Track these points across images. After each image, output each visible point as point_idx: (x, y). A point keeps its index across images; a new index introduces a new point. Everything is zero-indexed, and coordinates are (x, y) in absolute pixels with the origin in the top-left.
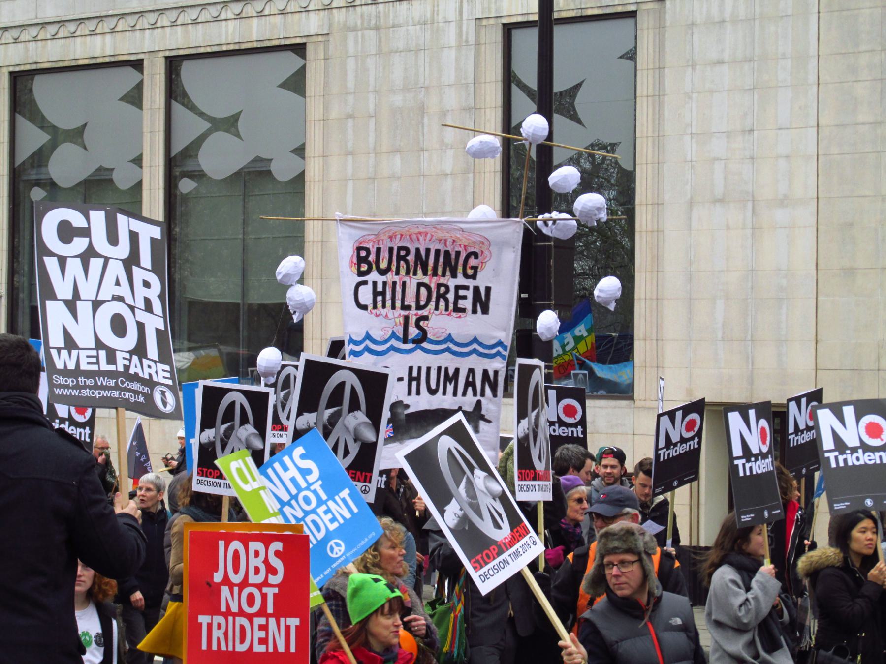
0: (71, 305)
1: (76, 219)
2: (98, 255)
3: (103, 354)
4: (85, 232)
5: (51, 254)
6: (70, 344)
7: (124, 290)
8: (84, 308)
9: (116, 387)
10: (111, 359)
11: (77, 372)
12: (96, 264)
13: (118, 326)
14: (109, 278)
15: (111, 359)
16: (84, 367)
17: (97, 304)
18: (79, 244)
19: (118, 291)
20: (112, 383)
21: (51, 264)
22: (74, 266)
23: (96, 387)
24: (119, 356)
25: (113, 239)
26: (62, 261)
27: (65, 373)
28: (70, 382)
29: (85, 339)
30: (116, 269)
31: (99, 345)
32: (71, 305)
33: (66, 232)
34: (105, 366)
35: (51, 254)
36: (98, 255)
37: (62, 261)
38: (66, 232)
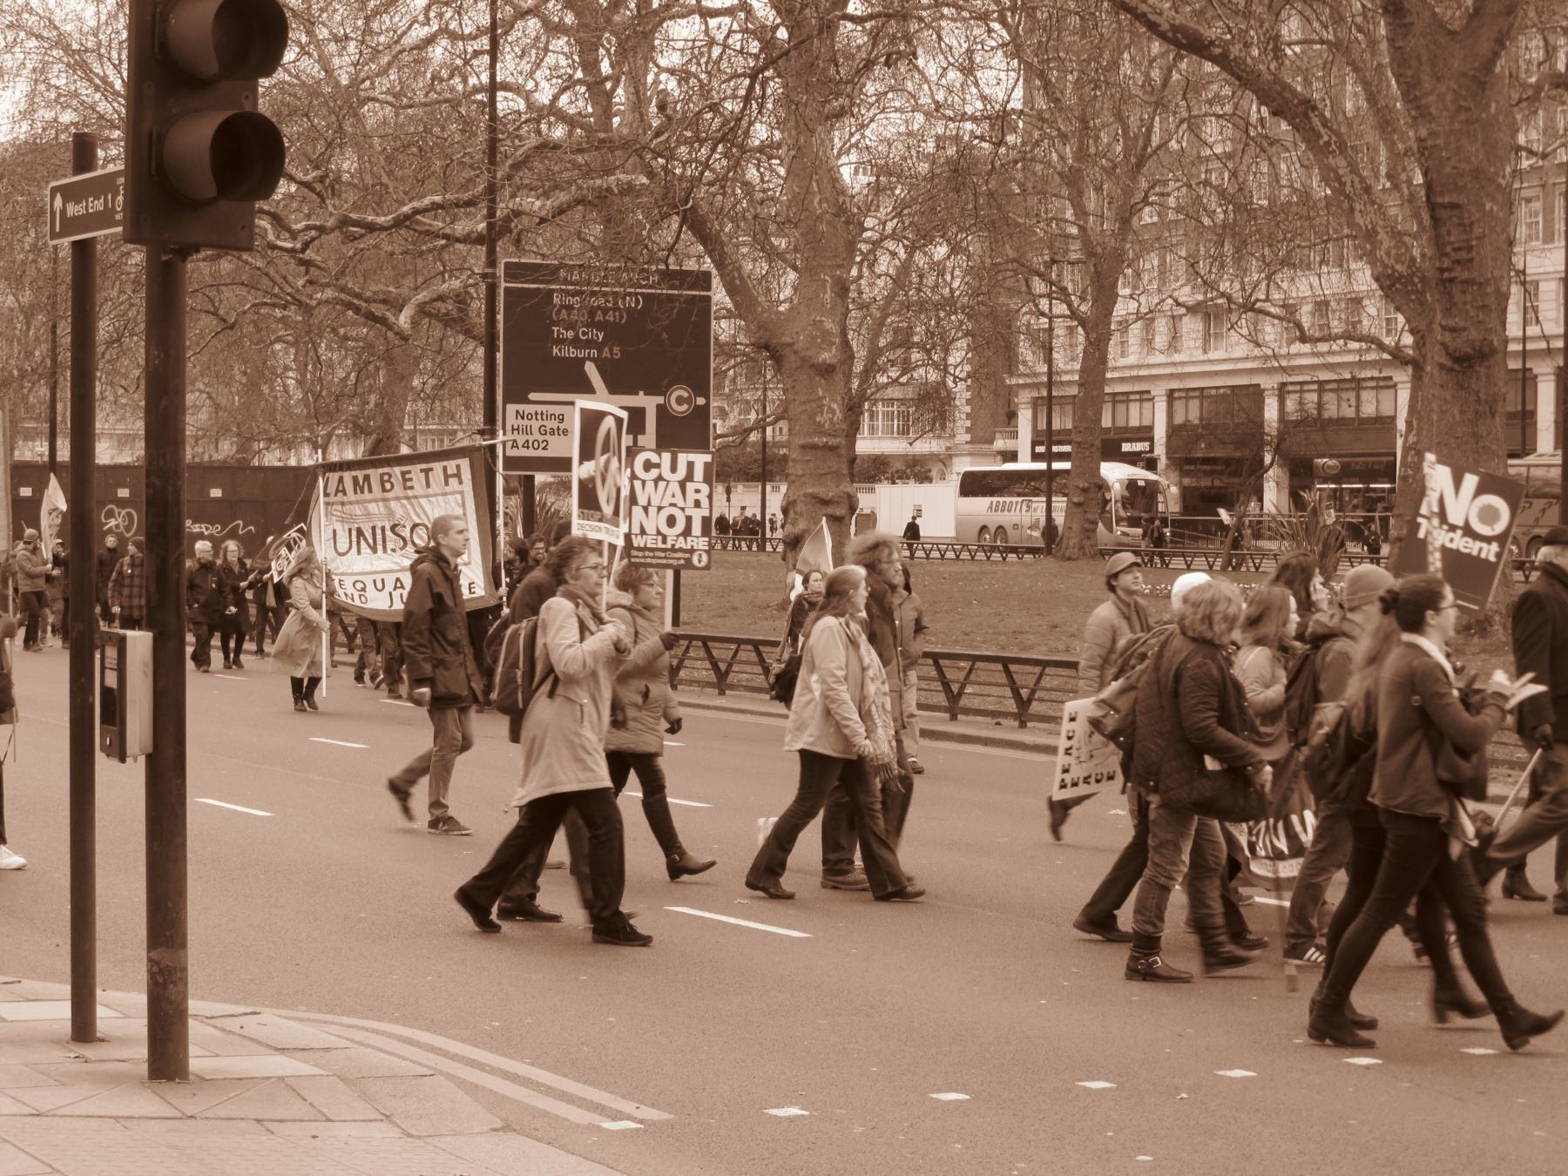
0: (646, 509)
1: (654, 458)
2: (664, 480)
3: (660, 538)
4: (658, 466)
5: (638, 478)
6: (643, 532)
7: (679, 500)
8: (653, 511)
9: (665, 558)
10: (664, 541)
11: (645, 549)
12: (662, 484)
13: (671, 521)
14: (669, 493)
15: (664, 541)
16: (649, 545)
17: (660, 508)
18: (654, 473)
19: (673, 501)
20: (663, 555)
21: (637, 484)
22: (650, 485)
23: (654, 557)
24: (669, 539)
25: (674, 469)
26: (644, 482)
27: (639, 549)
28: (641, 554)
29: (651, 529)
30: (675, 487)
31: (659, 533)
32: (646, 509)
33: (648, 466)
34: (661, 546)
35: (638, 478)
36: (664, 480)
37: (644, 482)
38: (648, 466)
